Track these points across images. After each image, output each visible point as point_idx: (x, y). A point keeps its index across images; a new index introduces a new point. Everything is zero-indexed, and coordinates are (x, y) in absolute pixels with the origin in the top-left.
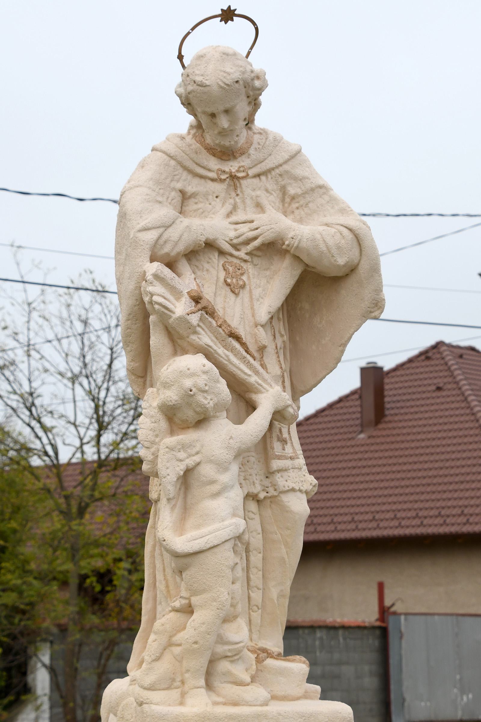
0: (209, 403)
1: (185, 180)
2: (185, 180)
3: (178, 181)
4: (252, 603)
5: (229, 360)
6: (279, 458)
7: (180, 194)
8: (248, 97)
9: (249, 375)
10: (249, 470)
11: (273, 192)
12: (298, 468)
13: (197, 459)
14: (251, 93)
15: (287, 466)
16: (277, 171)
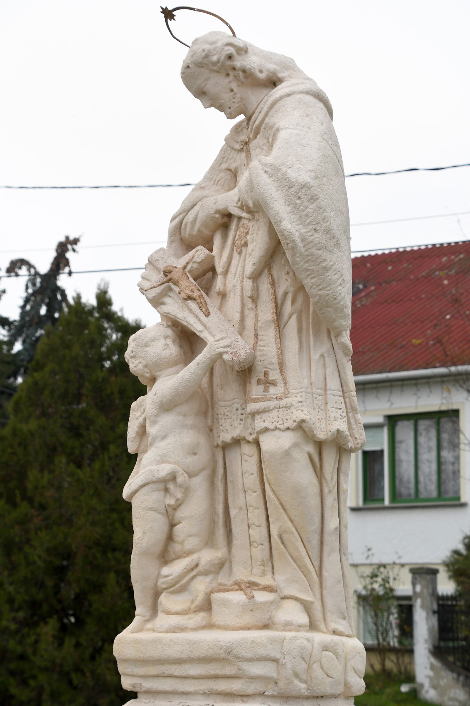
0: (135, 367)
1: (231, 159)
2: (231, 159)
3: (226, 162)
4: (252, 540)
5: (187, 322)
6: (255, 401)
7: (229, 172)
8: (218, 72)
9: (199, 331)
10: (233, 417)
11: (264, 147)
12: (285, 407)
13: (143, 416)
14: (215, 68)
15: (263, 407)
16: (263, 126)
